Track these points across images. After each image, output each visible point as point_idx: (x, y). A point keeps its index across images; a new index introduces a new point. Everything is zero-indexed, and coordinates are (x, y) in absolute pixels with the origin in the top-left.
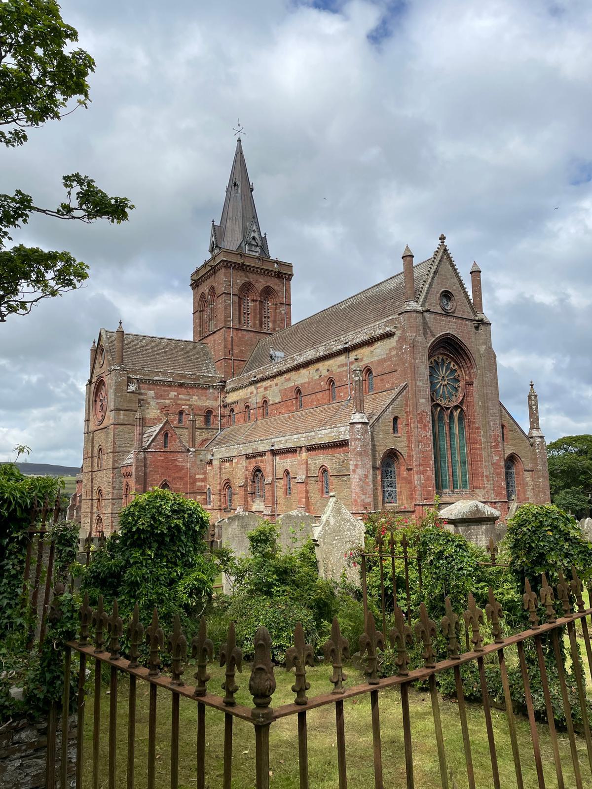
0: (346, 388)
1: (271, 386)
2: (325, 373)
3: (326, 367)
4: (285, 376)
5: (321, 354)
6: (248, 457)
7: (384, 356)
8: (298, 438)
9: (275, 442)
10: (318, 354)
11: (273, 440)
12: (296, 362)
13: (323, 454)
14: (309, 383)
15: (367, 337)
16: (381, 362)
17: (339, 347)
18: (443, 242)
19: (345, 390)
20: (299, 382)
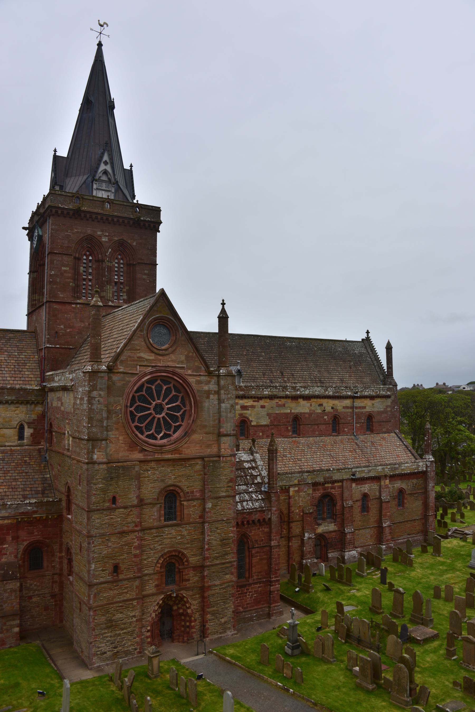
0: (351, 426)
1: (253, 407)
2: (328, 409)
3: (332, 405)
4: (277, 400)
5: (331, 393)
6: (315, 485)
7: (382, 410)
8: (383, 469)
9: (356, 472)
10: (327, 392)
11: (354, 470)
12: (299, 393)
13: (401, 479)
14: (310, 414)
15: (374, 394)
16: (380, 413)
17: (349, 393)
18: (368, 335)
19: (350, 427)
20: (297, 411)
